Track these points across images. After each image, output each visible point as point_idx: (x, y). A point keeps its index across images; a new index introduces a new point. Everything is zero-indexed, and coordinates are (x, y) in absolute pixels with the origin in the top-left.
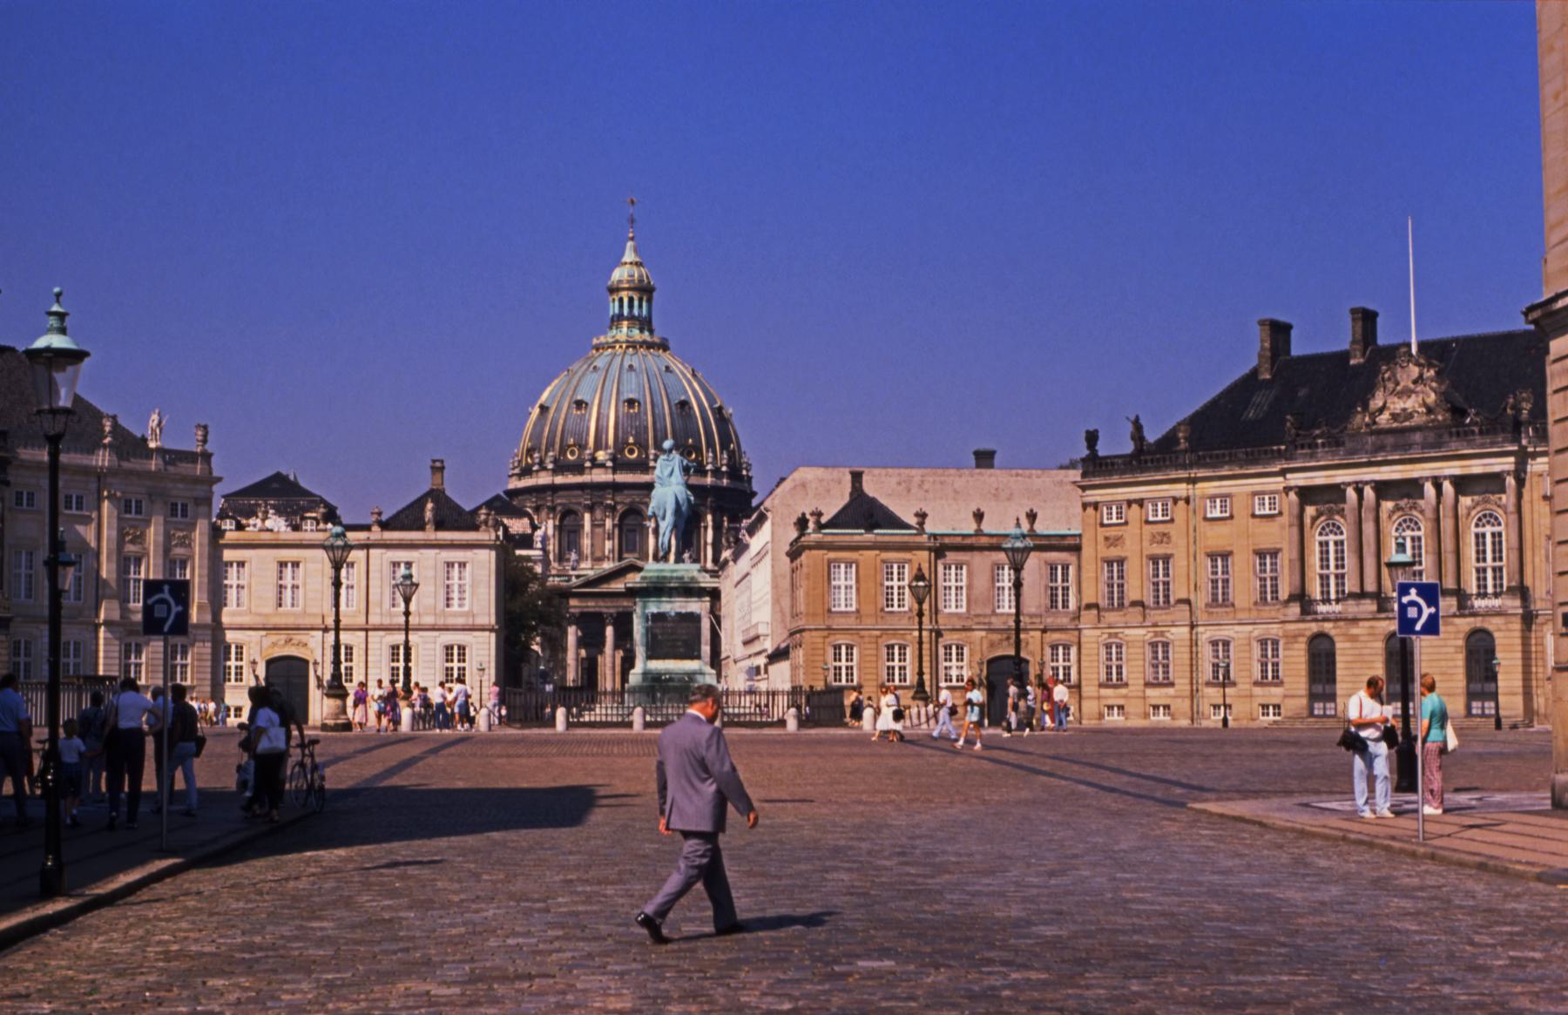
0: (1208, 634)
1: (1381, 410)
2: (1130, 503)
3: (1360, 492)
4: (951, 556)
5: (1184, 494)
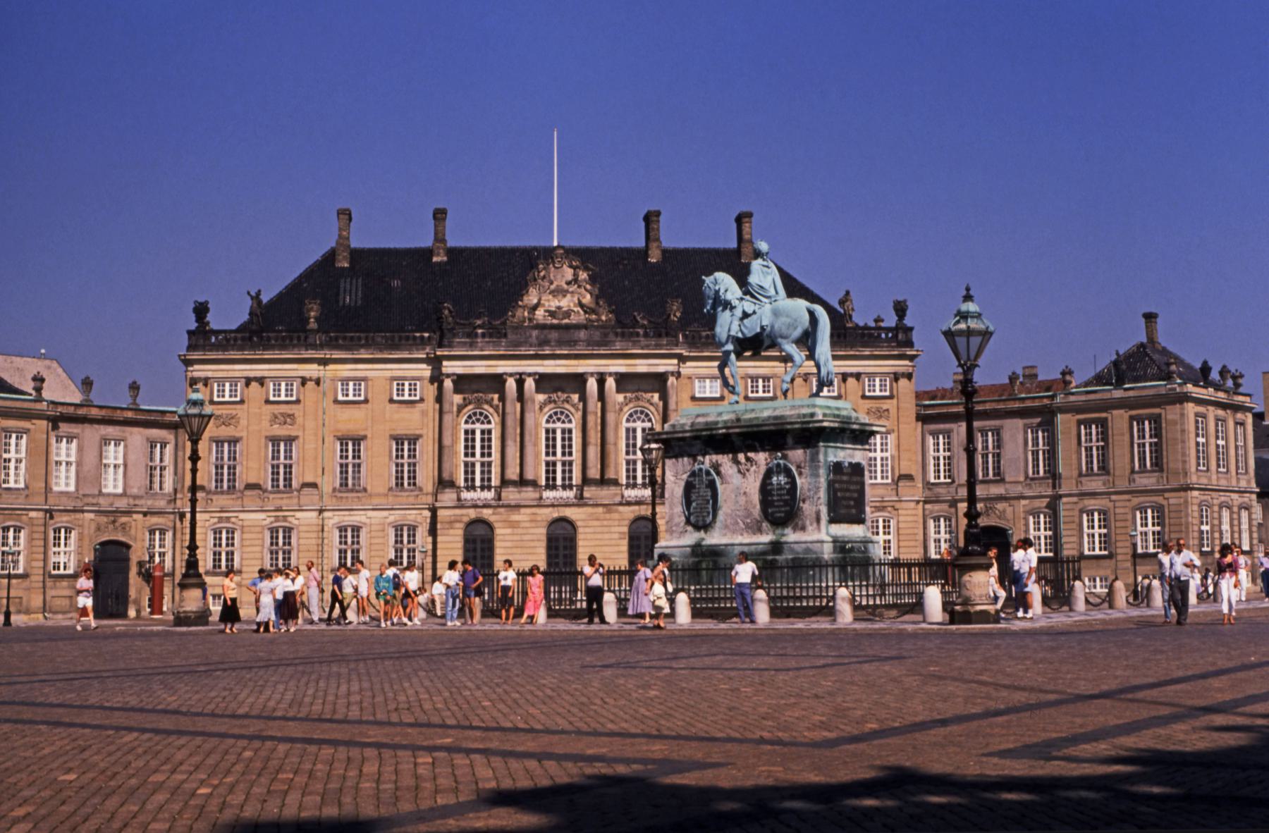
0: (336, 520)
1: (535, 308)
2: (248, 381)
3: (520, 383)
4: (64, 428)
5: (315, 375)
